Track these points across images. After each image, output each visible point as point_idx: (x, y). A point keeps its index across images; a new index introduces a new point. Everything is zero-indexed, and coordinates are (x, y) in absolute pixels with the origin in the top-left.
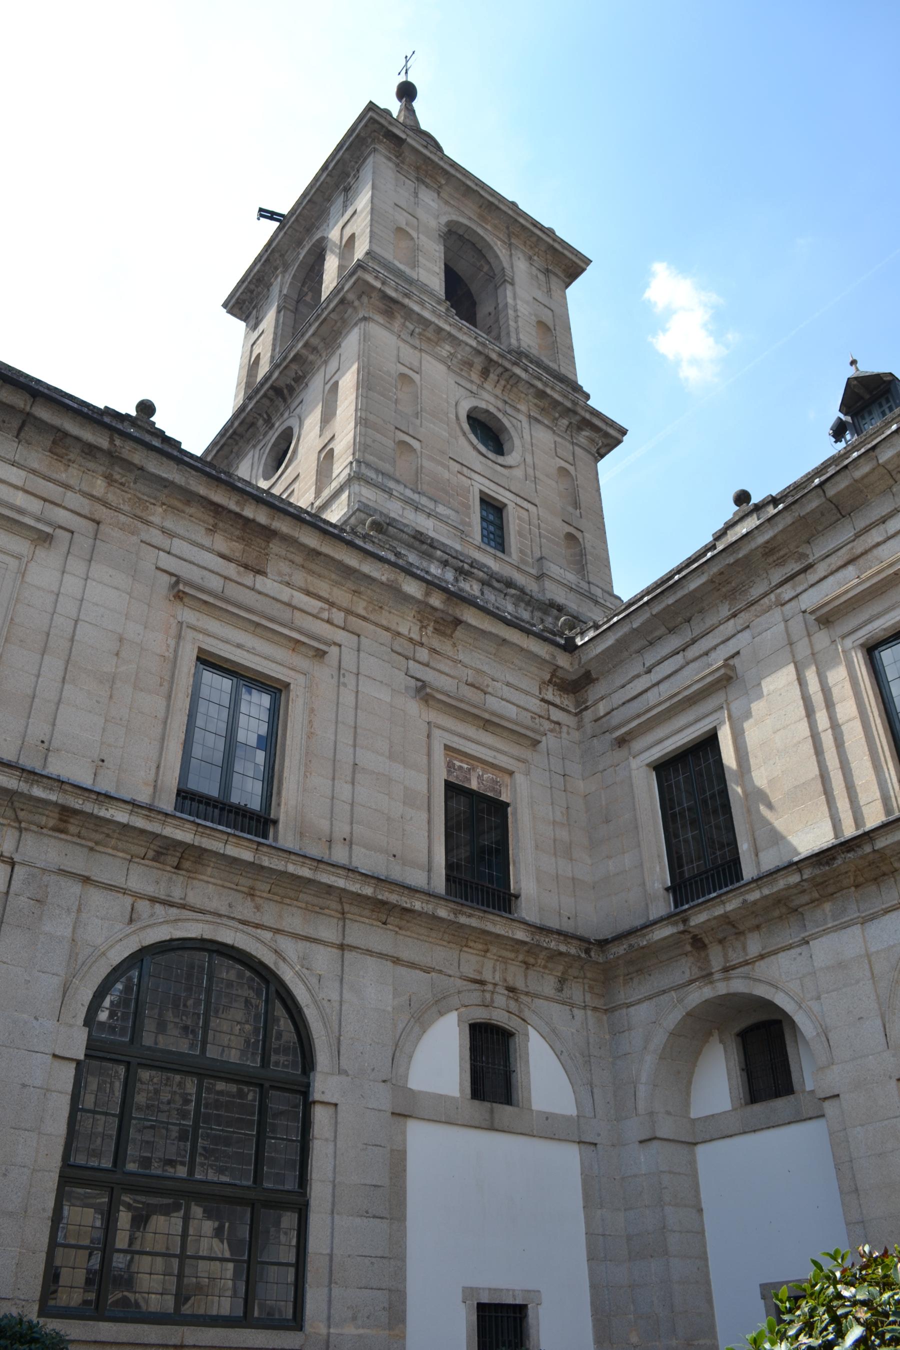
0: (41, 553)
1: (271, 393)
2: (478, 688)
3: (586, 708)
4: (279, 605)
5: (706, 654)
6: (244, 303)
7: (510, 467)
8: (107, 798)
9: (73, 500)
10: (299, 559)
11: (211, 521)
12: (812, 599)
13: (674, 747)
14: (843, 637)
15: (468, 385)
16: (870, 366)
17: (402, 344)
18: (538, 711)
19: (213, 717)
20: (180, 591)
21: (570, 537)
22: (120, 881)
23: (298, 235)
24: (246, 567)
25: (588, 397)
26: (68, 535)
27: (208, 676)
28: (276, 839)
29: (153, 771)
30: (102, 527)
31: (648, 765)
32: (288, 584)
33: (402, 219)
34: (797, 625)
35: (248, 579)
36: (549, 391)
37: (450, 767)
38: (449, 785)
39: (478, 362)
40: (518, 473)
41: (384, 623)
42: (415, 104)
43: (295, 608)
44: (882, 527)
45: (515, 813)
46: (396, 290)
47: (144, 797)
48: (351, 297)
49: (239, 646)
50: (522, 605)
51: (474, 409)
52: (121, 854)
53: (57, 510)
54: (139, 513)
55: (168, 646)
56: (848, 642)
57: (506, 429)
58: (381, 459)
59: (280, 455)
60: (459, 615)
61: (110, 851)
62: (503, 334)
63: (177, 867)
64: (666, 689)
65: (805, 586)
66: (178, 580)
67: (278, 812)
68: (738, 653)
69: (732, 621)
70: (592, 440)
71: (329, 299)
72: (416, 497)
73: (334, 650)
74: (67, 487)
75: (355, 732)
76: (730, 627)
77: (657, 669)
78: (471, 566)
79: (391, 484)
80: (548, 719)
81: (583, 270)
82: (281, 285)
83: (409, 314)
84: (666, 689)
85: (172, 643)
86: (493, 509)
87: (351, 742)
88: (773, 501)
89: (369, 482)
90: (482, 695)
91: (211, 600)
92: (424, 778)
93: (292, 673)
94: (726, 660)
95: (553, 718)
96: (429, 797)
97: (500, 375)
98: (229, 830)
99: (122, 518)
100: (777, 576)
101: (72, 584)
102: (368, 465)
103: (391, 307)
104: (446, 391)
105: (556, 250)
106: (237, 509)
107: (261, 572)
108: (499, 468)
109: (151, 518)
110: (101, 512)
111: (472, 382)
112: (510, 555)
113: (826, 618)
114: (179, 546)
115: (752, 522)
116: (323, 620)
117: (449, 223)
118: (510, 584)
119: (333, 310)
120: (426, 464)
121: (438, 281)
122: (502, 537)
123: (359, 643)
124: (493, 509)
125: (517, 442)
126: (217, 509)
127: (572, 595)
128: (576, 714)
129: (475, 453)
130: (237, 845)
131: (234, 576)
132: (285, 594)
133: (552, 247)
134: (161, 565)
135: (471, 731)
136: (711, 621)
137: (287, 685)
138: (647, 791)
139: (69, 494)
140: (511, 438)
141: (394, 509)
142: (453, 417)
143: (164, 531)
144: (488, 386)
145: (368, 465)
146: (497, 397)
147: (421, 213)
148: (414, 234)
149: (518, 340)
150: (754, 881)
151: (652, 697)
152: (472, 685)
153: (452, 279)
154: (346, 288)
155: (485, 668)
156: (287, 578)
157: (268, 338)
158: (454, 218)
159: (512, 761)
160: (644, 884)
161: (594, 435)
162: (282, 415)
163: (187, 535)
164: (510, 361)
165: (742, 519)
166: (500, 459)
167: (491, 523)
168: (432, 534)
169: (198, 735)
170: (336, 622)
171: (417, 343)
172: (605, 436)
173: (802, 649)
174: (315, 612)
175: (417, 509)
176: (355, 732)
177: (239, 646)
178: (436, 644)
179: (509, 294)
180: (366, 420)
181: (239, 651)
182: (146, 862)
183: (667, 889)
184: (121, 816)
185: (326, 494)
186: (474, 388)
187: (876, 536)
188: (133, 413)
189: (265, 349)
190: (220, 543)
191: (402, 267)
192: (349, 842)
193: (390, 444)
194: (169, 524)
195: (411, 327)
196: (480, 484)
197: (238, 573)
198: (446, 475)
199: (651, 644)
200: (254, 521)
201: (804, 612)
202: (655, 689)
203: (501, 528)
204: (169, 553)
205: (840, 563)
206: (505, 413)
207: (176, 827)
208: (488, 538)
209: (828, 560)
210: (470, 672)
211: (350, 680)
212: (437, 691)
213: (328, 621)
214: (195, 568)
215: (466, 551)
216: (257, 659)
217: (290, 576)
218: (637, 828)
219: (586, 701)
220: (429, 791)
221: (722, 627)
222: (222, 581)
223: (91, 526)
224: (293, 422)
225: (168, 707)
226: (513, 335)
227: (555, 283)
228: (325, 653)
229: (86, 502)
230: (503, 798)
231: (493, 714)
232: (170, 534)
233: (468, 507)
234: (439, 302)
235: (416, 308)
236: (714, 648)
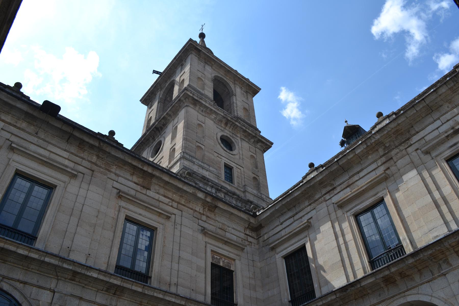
0: (73, 181)
1: (155, 129)
2: (223, 230)
3: (260, 237)
4: (154, 200)
5: (301, 218)
6: (147, 100)
7: (235, 155)
8: (90, 268)
9: (85, 163)
10: (162, 185)
11: (132, 171)
12: (336, 199)
13: (291, 250)
14: (347, 212)
15: (221, 128)
16: (352, 123)
17: (199, 114)
18: (244, 238)
19: (130, 239)
20: (120, 195)
21: (254, 178)
22: (93, 299)
23: (166, 79)
24: (144, 187)
25: (260, 132)
26: (82, 175)
27: (128, 225)
28: (150, 284)
29: (107, 259)
30: (94, 173)
31: (282, 257)
32: (158, 193)
33: (200, 75)
34: (331, 208)
35: (144, 191)
36: (247, 130)
37: (213, 257)
38: (212, 264)
39: (224, 120)
40: (237, 157)
41: (191, 207)
42: (205, 40)
43: (160, 201)
44: (358, 175)
45: (235, 275)
46: (197, 97)
47: (103, 268)
48: (182, 99)
49: (140, 214)
50: (238, 201)
51: (223, 136)
52: (94, 289)
53: (79, 166)
54: (107, 168)
55: (115, 214)
56: (349, 214)
57: (233, 142)
58: (191, 151)
59: (157, 150)
60: (216, 204)
61: (90, 288)
62: (232, 112)
63: (114, 294)
64: (288, 230)
65: (333, 195)
66: (120, 191)
67: (151, 274)
68: (312, 217)
69: (309, 207)
70: (261, 146)
71: (175, 99)
72: (203, 164)
73: (173, 216)
74: (83, 159)
75: (180, 245)
76: (309, 209)
77: (284, 223)
78: (221, 188)
79: (194, 160)
80: (247, 241)
81: (258, 92)
82: (159, 94)
83: (201, 105)
84: (288, 230)
85: (117, 213)
86: (229, 169)
87: (178, 249)
88: (322, 166)
89: (187, 159)
90: (224, 232)
91: (131, 198)
92: (204, 262)
93: (158, 224)
94: (308, 220)
95: (249, 240)
96: (205, 269)
97: (231, 125)
98: (134, 280)
99: (102, 170)
100: (324, 191)
101: (83, 192)
102: (187, 154)
103: (195, 102)
104: (213, 129)
105: (250, 85)
106: (141, 167)
107: (149, 189)
108: (230, 155)
109: (112, 170)
110: (95, 167)
111: (222, 127)
112: (234, 184)
113: (341, 205)
114: (121, 180)
115: (315, 173)
116: (169, 206)
117: (215, 76)
118: (234, 194)
119: (176, 103)
122: (232, 178)
123: (182, 214)
124: (229, 169)
125: (237, 147)
126: (135, 167)
127: (255, 198)
128: (257, 239)
129: (223, 150)
130: (136, 286)
131: (139, 190)
132: (157, 196)
133: (248, 84)
134: (114, 186)
135: (220, 245)
136: (302, 206)
137: (156, 228)
138: (282, 266)
139: (84, 161)
140: (235, 145)
141: (195, 168)
143: (116, 174)
144: (227, 128)
145: (187, 154)
146: (230, 132)
147: (205, 73)
148: (204, 80)
149: (237, 113)
150: (320, 298)
151: (283, 233)
152: (221, 229)
153: (216, 93)
154: (181, 96)
155: (225, 223)
156: (158, 191)
157: (155, 111)
158: (217, 75)
159: (235, 256)
160: (281, 300)
161: (262, 145)
162: (158, 136)
163: (124, 176)
164: (234, 120)
165: (311, 172)
166: (231, 152)
167: (228, 173)
168: (208, 177)
169: (124, 245)
170: (174, 206)
171: (204, 114)
172: (266, 145)
173: (333, 216)
174: (167, 203)
175: (203, 168)
176: (180, 245)
177: (140, 214)
178: (208, 214)
179: (234, 99)
180: (186, 139)
181: (140, 216)
182: (103, 292)
183: (289, 302)
184: (95, 275)
185: (172, 163)
186: (223, 129)
187: (356, 178)
188: (108, 135)
189: (153, 115)
190: (135, 179)
191: (199, 90)
192: (177, 285)
194: (118, 172)
195: (202, 109)
196: (224, 160)
197: (141, 189)
198: (213, 157)
199: (282, 214)
200: (147, 171)
201: (333, 203)
202: (284, 230)
203: (231, 175)
204: (117, 182)
205: (345, 187)
206: (233, 137)
207: (115, 279)
208: (227, 178)
209: (341, 186)
210: (220, 224)
211: (178, 227)
212: (209, 231)
213: (172, 206)
214: (126, 187)
215: (219, 183)
216: (146, 219)
217: (159, 190)
218: (278, 279)
219: (260, 234)
220: (205, 267)
221: (306, 209)
222: (135, 192)
223: (90, 172)
224: (162, 139)
225: (114, 236)
226: (236, 112)
227: (249, 96)
228: (170, 217)
229: (89, 164)
230: (232, 269)
231: (228, 239)
232: (118, 176)
233: (220, 168)
234: (211, 101)
235: (204, 103)
236: (304, 216)
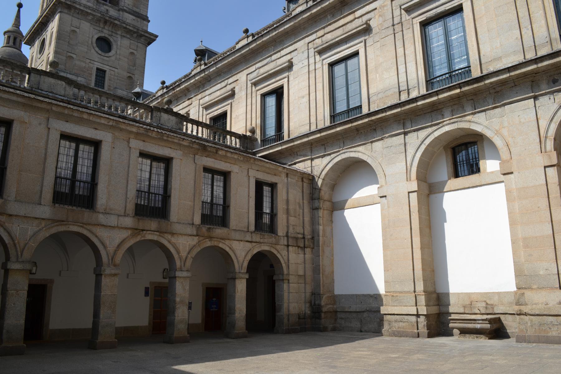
21: (130, 77)
36: (128, 27)
40: (113, 58)
48: (56, 3)
70: (145, 40)
83: (76, 8)
86: (101, 73)
108: (105, 58)
120: (77, 63)
124: (101, 73)
144: (106, 28)
146: (109, 31)
193: (64, 58)
235: (78, 6)
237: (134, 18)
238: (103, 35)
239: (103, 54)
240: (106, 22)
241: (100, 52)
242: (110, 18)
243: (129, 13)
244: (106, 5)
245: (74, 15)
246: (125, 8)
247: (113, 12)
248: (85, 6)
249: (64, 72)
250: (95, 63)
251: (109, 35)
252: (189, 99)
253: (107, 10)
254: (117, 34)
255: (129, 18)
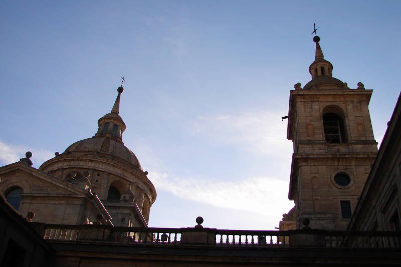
36: (358, 156)
40: (353, 188)
42: (319, 42)
103: (306, 160)
121: (321, 136)
142: (330, 182)
144: (340, 164)
146: (343, 166)
148: (313, 123)
158: (325, 106)
196: (340, 198)
237: (363, 146)
238: (339, 171)
239: (343, 187)
240: (338, 159)
241: (340, 187)
242: (341, 155)
243: (357, 144)
244: (336, 146)
245: (312, 164)
246: (352, 141)
247: (343, 149)
248: (317, 154)
249: (314, 214)
250: (339, 197)
251: (344, 169)
252: (373, 208)
253: (338, 149)
254: (351, 166)
255: (358, 148)
